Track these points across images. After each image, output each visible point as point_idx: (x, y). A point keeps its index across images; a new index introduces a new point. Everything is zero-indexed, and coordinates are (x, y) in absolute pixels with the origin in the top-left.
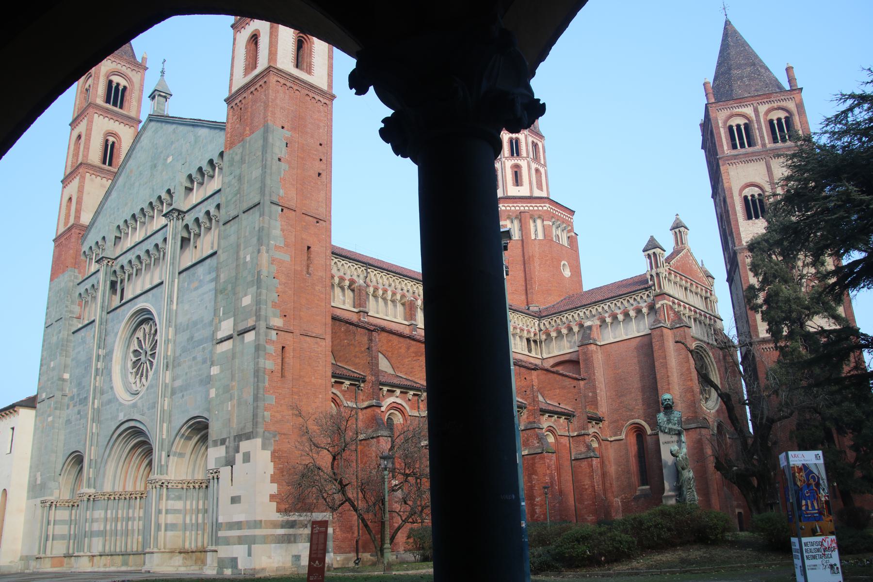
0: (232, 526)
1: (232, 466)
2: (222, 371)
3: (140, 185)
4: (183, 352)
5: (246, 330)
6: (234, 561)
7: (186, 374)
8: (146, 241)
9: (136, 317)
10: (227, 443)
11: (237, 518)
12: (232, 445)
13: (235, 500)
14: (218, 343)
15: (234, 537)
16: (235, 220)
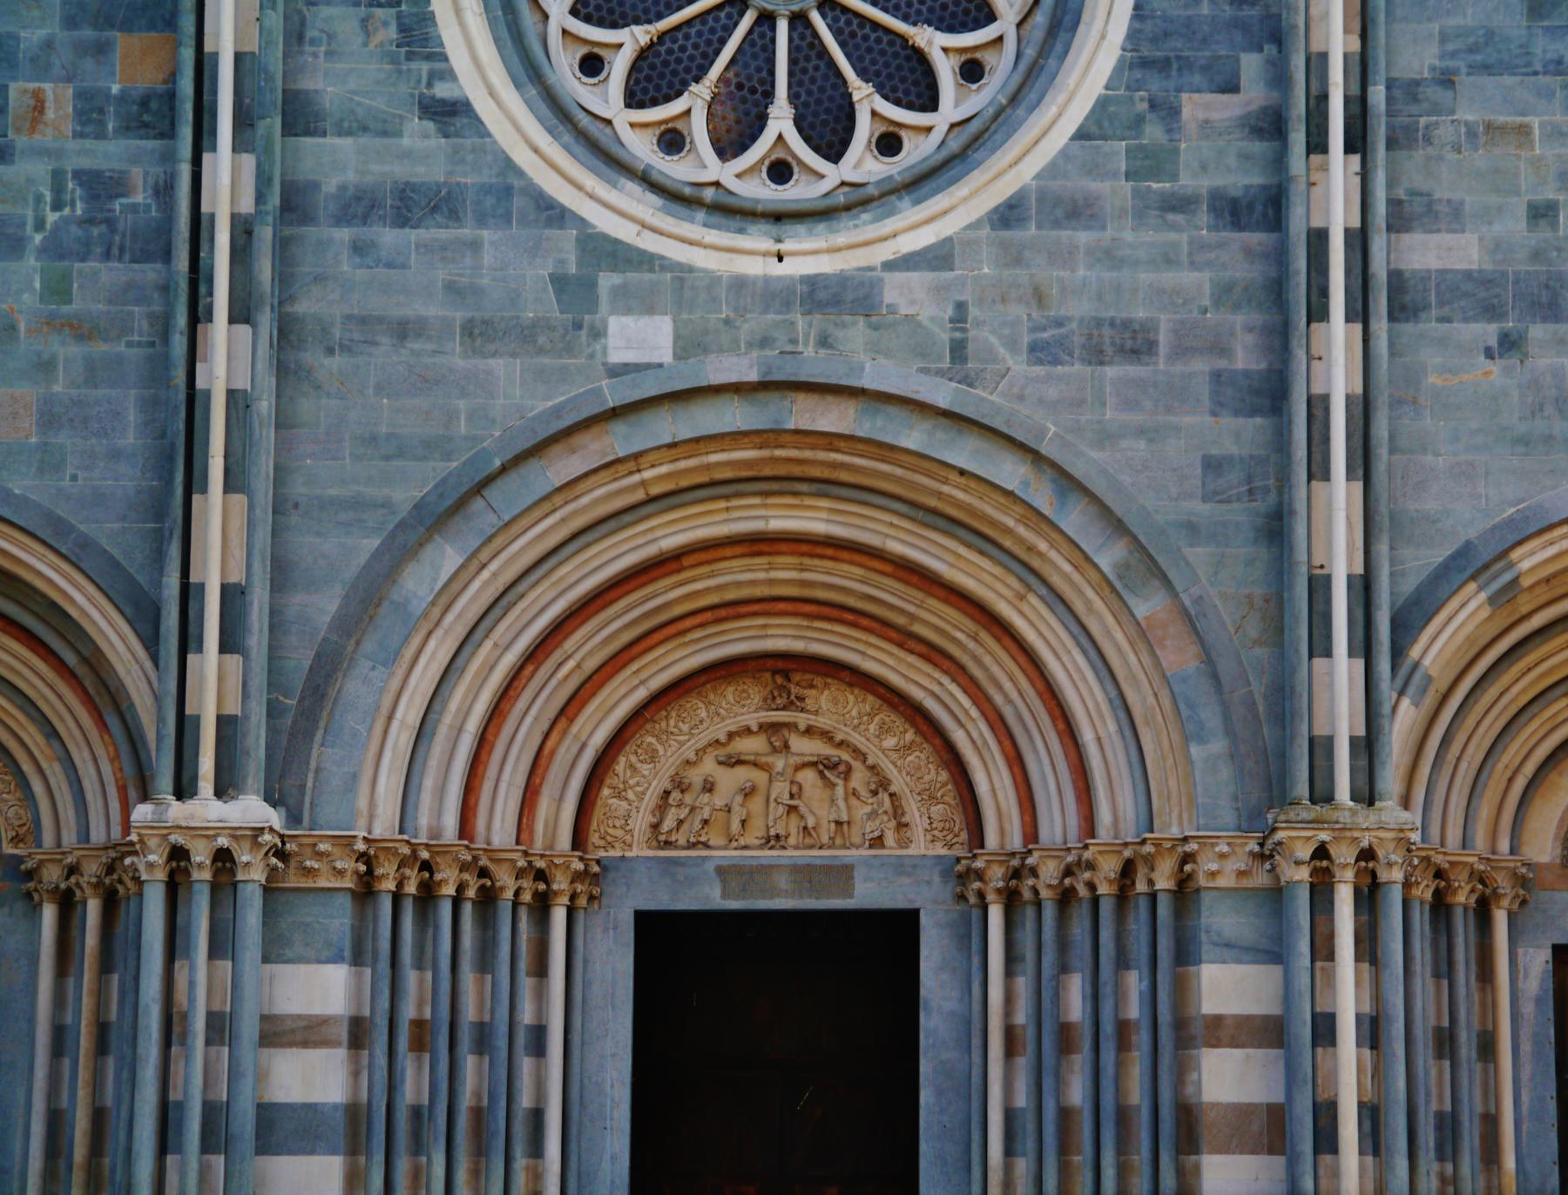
4: (1486, 69)
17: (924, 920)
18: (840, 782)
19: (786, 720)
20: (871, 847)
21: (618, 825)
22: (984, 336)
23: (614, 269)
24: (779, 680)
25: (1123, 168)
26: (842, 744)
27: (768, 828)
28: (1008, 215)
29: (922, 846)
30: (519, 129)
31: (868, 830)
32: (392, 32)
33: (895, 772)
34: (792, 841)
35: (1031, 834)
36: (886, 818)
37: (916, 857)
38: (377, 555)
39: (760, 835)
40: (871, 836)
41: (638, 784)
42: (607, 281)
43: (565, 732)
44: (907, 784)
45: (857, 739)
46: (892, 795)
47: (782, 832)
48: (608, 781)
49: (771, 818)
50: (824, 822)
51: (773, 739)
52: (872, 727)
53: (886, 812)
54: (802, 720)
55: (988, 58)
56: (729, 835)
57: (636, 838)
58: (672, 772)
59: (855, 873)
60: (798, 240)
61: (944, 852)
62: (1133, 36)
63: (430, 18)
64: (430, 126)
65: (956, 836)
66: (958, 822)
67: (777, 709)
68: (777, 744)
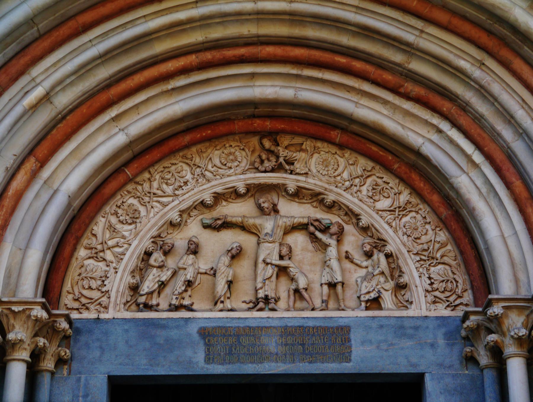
17: (429, 384)
18: (333, 242)
19: (275, 181)
20: (367, 308)
21: (94, 287)
24: (267, 144)
26: (331, 207)
27: (256, 291)
29: (424, 307)
31: (364, 291)
33: (390, 231)
34: (282, 304)
36: (382, 279)
37: (418, 318)
39: (247, 299)
40: (367, 297)
41: (117, 245)
43: (34, 175)
44: (404, 245)
46: (388, 256)
47: (271, 294)
48: (85, 241)
49: (259, 279)
50: (316, 287)
51: (261, 201)
52: (364, 189)
53: (382, 273)
56: (214, 297)
57: (113, 299)
58: (154, 232)
59: (352, 336)
61: (447, 313)
65: (459, 297)
66: (460, 281)
67: (265, 171)
68: (266, 205)
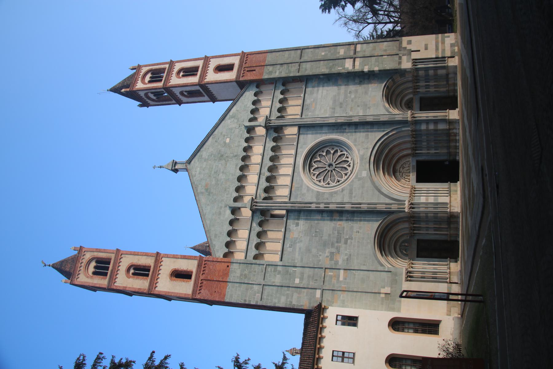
0: (437, 49)
1: (413, 51)
2: (368, 65)
3: (223, 172)
4: (346, 110)
5: (355, 49)
6: (452, 45)
7: (358, 106)
8: (263, 160)
9: (305, 170)
10: (400, 55)
11: (434, 47)
12: (402, 52)
13: (426, 49)
14: (354, 68)
15: (442, 47)
16: (300, 65)
17: (417, 159)
22: (366, 147)
23: (358, 176)
25: (351, 137)
28: (355, 145)
30: (344, 184)
32: (335, 195)
35: (409, 148)
38: (383, 195)
42: (359, 176)
45: (400, 165)
54: (398, 170)
55: (341, 150)
60: (356, 162)
62: (340, 136)
63: (334, 191)
64: (344, 191)
